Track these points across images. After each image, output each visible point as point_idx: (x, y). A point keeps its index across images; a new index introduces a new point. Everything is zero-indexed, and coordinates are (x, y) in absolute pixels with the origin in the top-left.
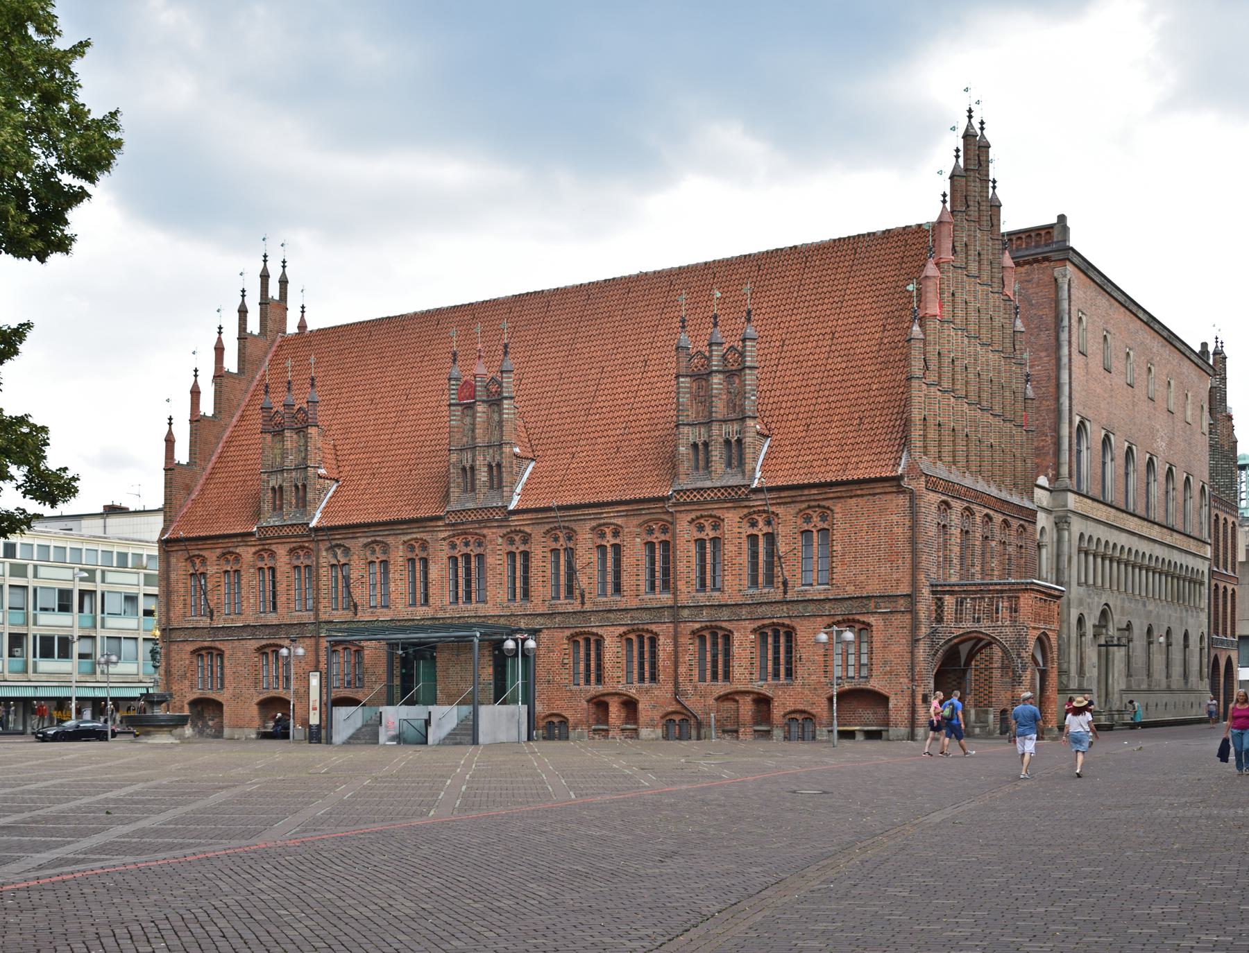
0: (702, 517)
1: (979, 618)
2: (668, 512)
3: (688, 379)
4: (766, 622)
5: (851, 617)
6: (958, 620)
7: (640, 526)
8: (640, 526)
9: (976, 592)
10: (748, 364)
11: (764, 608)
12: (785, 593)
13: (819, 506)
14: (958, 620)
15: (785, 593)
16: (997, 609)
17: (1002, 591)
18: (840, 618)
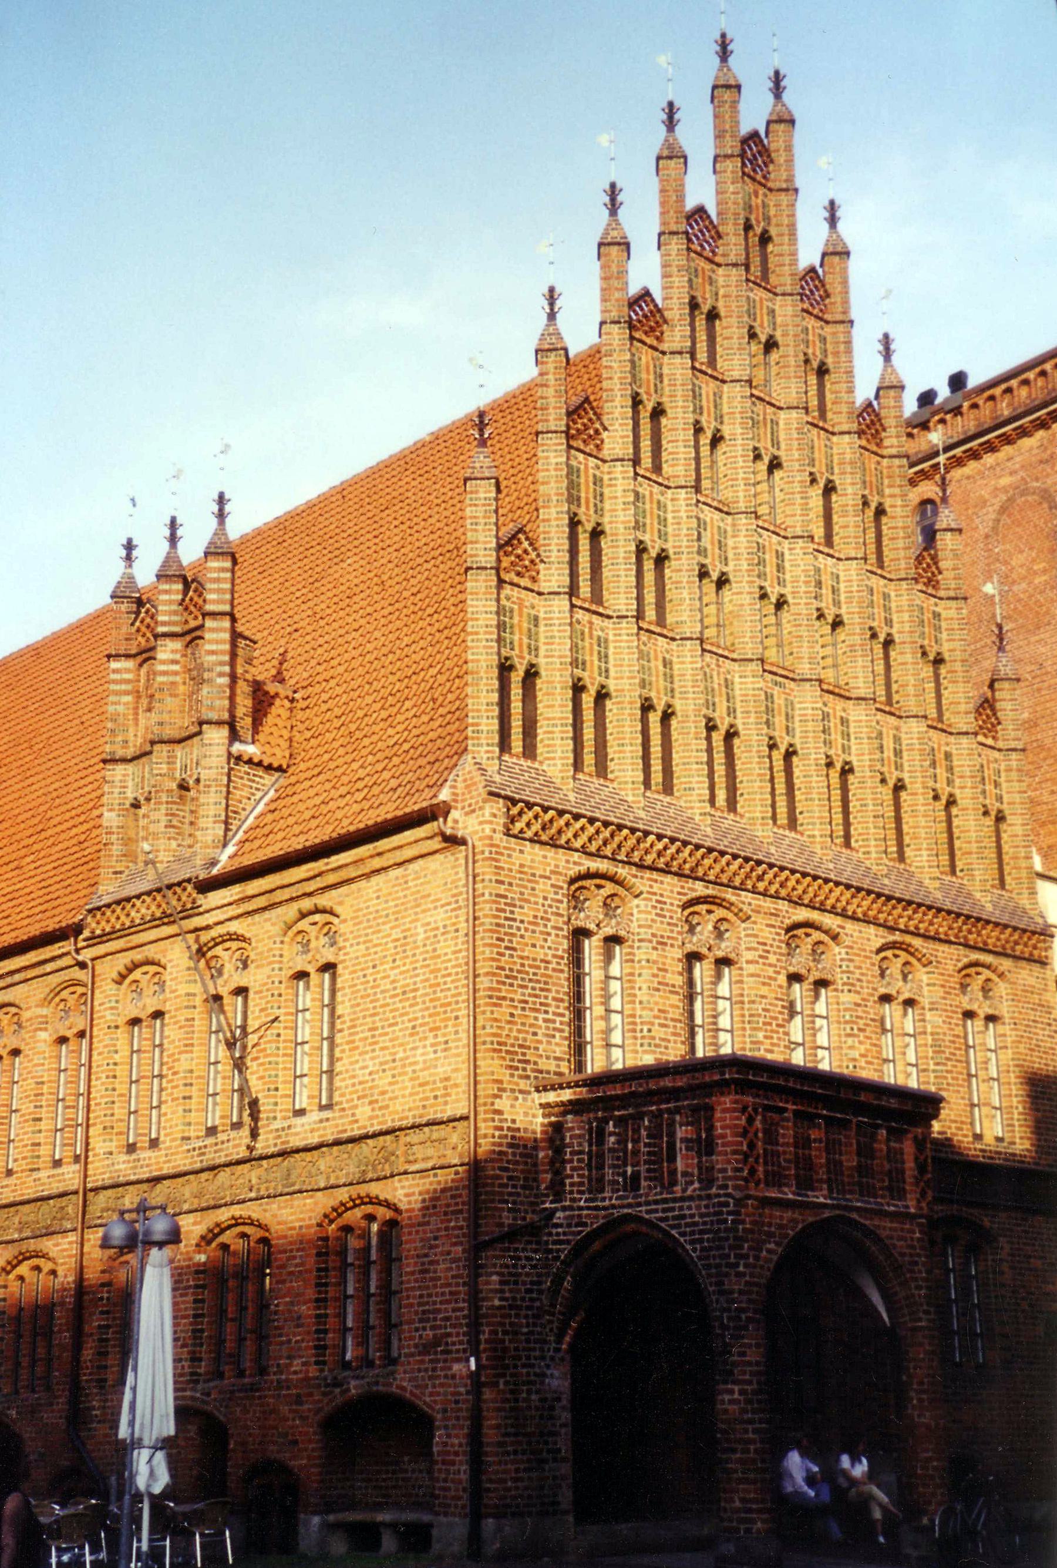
0: (136, 966)
1: (636, 1177)
2: (82, 965)
3: (130, 664)
4: (224, 1215)
5: (363, 1190)
6: (597, 1186)
7: (47, 1001)
8: (47, 1001)
9: (623, 1101)
10: (209, 607)
11: (224, 1176)
12: (254, 1134)
13: (317, 911)
14: (597, 1186)
15: (254, 1134)
16: (671, 1146)
17: (674, 1094)
18: (343, 1195)
